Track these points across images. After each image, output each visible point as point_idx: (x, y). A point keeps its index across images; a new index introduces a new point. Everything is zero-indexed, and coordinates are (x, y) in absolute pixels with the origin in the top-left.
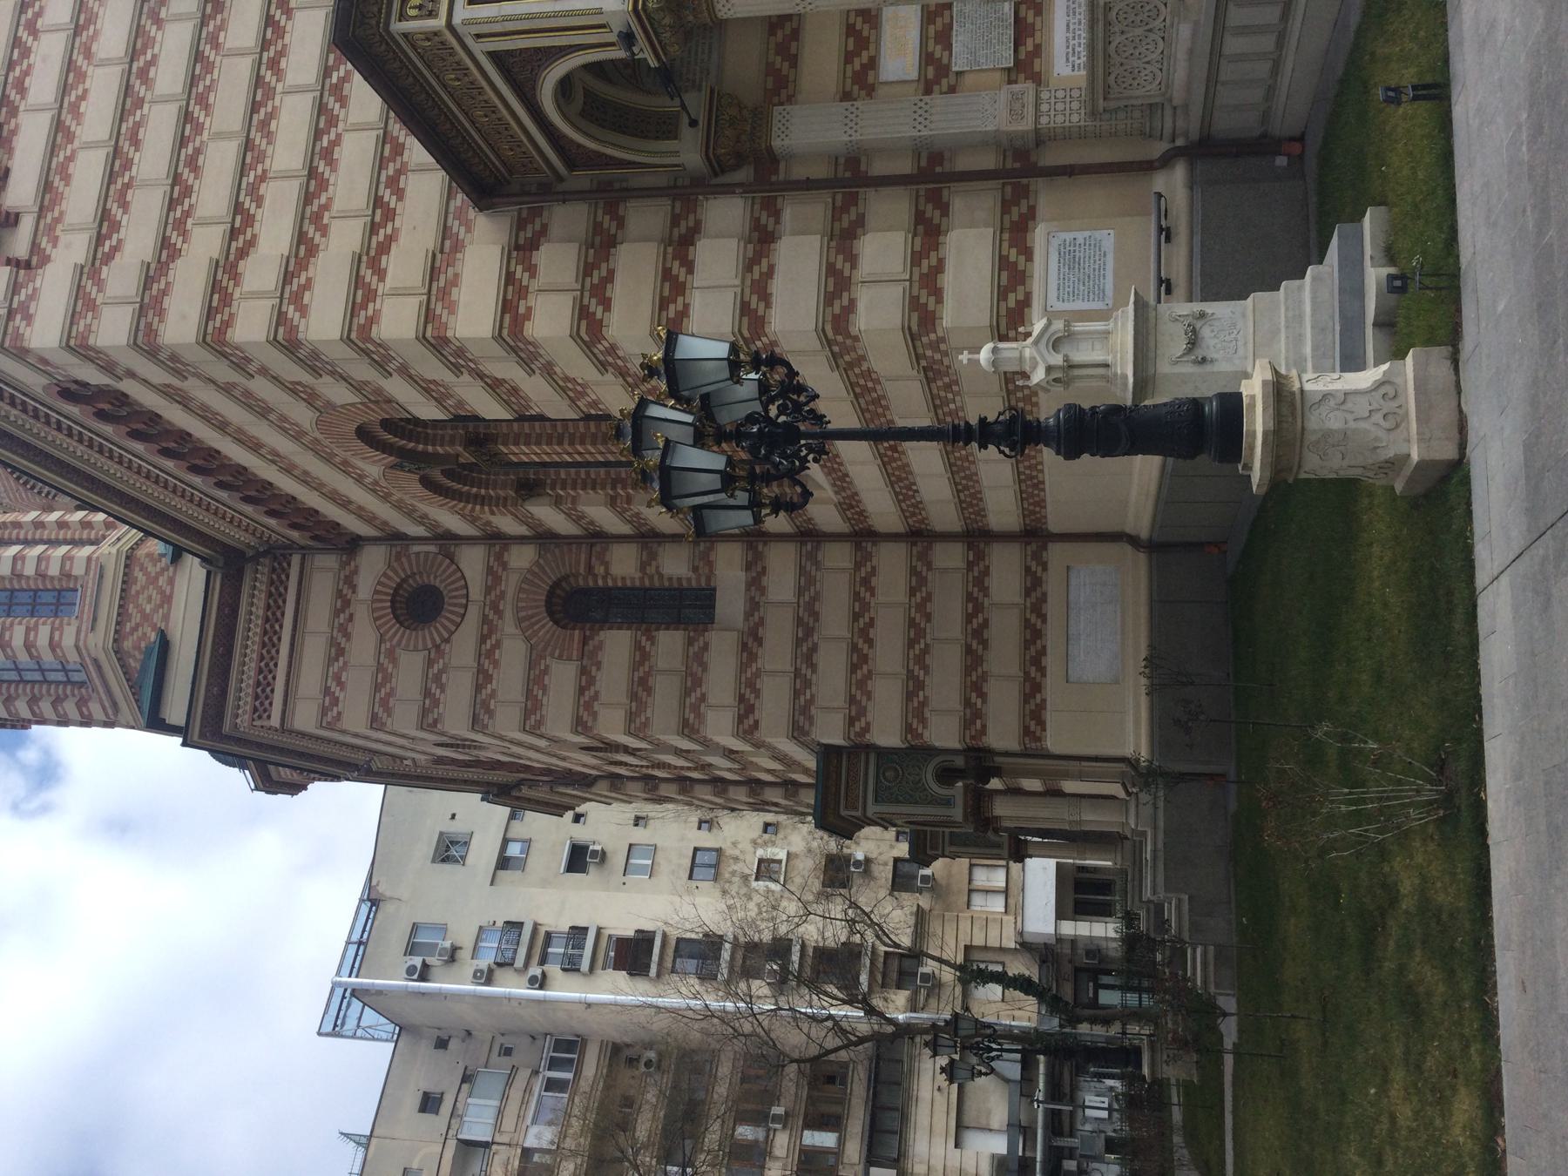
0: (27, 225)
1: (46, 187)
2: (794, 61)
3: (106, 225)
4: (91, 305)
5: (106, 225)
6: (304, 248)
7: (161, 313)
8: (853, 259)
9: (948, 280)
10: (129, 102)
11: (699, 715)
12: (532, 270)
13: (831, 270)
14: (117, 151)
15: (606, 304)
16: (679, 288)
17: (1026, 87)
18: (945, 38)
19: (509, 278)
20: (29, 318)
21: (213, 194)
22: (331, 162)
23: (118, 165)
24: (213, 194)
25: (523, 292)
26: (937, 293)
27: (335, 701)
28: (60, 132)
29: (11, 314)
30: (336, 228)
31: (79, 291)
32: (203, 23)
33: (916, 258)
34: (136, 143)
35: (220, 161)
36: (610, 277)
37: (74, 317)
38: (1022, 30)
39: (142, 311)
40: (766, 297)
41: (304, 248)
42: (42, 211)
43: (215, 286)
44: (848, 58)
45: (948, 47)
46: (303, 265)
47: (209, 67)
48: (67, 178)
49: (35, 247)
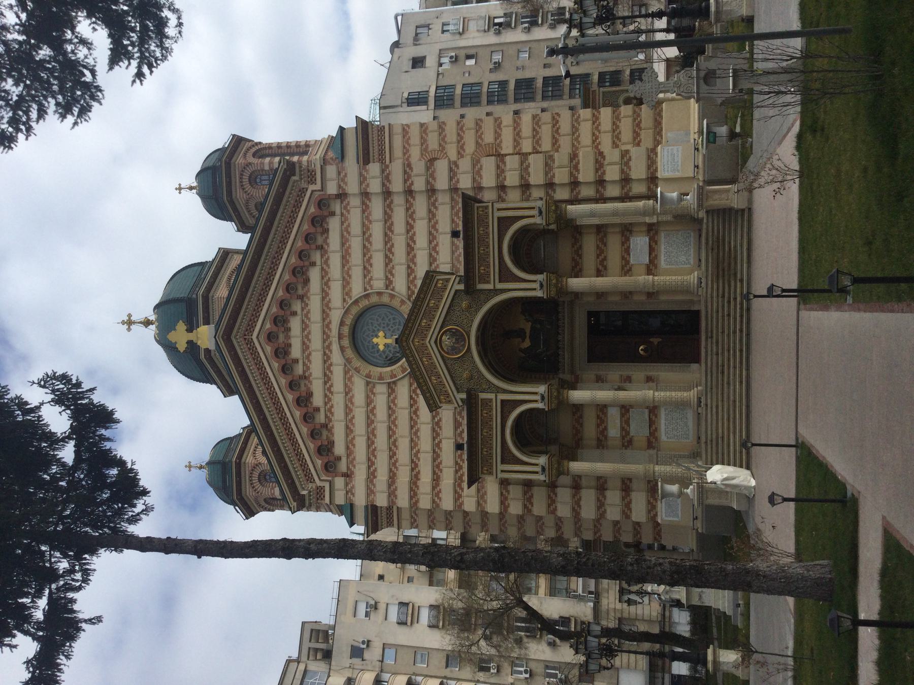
0: (344, 460)
1: (348, 448)
2: (581, 425)
3: (370, 463)
4: (372, 492)
5: (370, 463)
6: (436, 480)
7: (396, 497)
8: (605, 497)
9: (633, 506)
10: (370, 422)
11: (543, 530)
12: (508, 492)
13: (598, 500)
14: (368, 438)
15: (532, 504)
16: (553, 502)
17: (652, 452)
18: (627, 422)
19: (502, 494)
20: (353, 494)
21: (404, 455)
22: (440, 449)
23: (370, 443)
24: (404, 455)
25: (506, 499)
26: (630, 510)
27: (415, 521)
28: (349, 430)
29: (347, 493)
30: (445, 470)
31: (368, 488)
32: (389, 396)
33: (623, 499)
34: (375, 436)
35: (404, 445)
36: (532, 496)
37: (368, 495)
38: (651, 423)
39: (389, 496)
40: (580, 506)
41: (436, 480)
42: (348, 456)
43: (411, 489)
44: (598, 426)
45: (629, 425)
46: (438, 485)
47: (394, 412)
48: (354, 445)
49: (348, 468)
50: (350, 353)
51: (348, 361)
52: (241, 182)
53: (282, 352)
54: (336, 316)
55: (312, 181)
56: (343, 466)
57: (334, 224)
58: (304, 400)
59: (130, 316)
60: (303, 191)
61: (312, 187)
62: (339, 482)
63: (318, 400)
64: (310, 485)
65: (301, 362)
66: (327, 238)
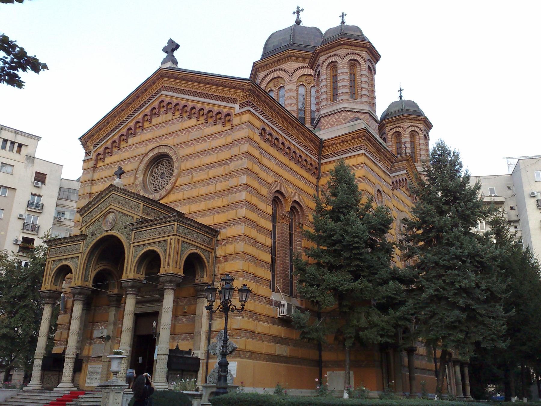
50: (151, 155)
51: (147, 154)
52: (330, 56)
53: (155, 112)
54: (170, 141)
55: (242, 106)
56: (100, 164)
57: (219, 127)
58: (131, 132)
59: (302, 10)
60: (234, 101)
61: (237, 107)
62: (91, 164)
63: (131, 141)
64: (92, 147)
65: (150, 125)
66: (212, 125)
